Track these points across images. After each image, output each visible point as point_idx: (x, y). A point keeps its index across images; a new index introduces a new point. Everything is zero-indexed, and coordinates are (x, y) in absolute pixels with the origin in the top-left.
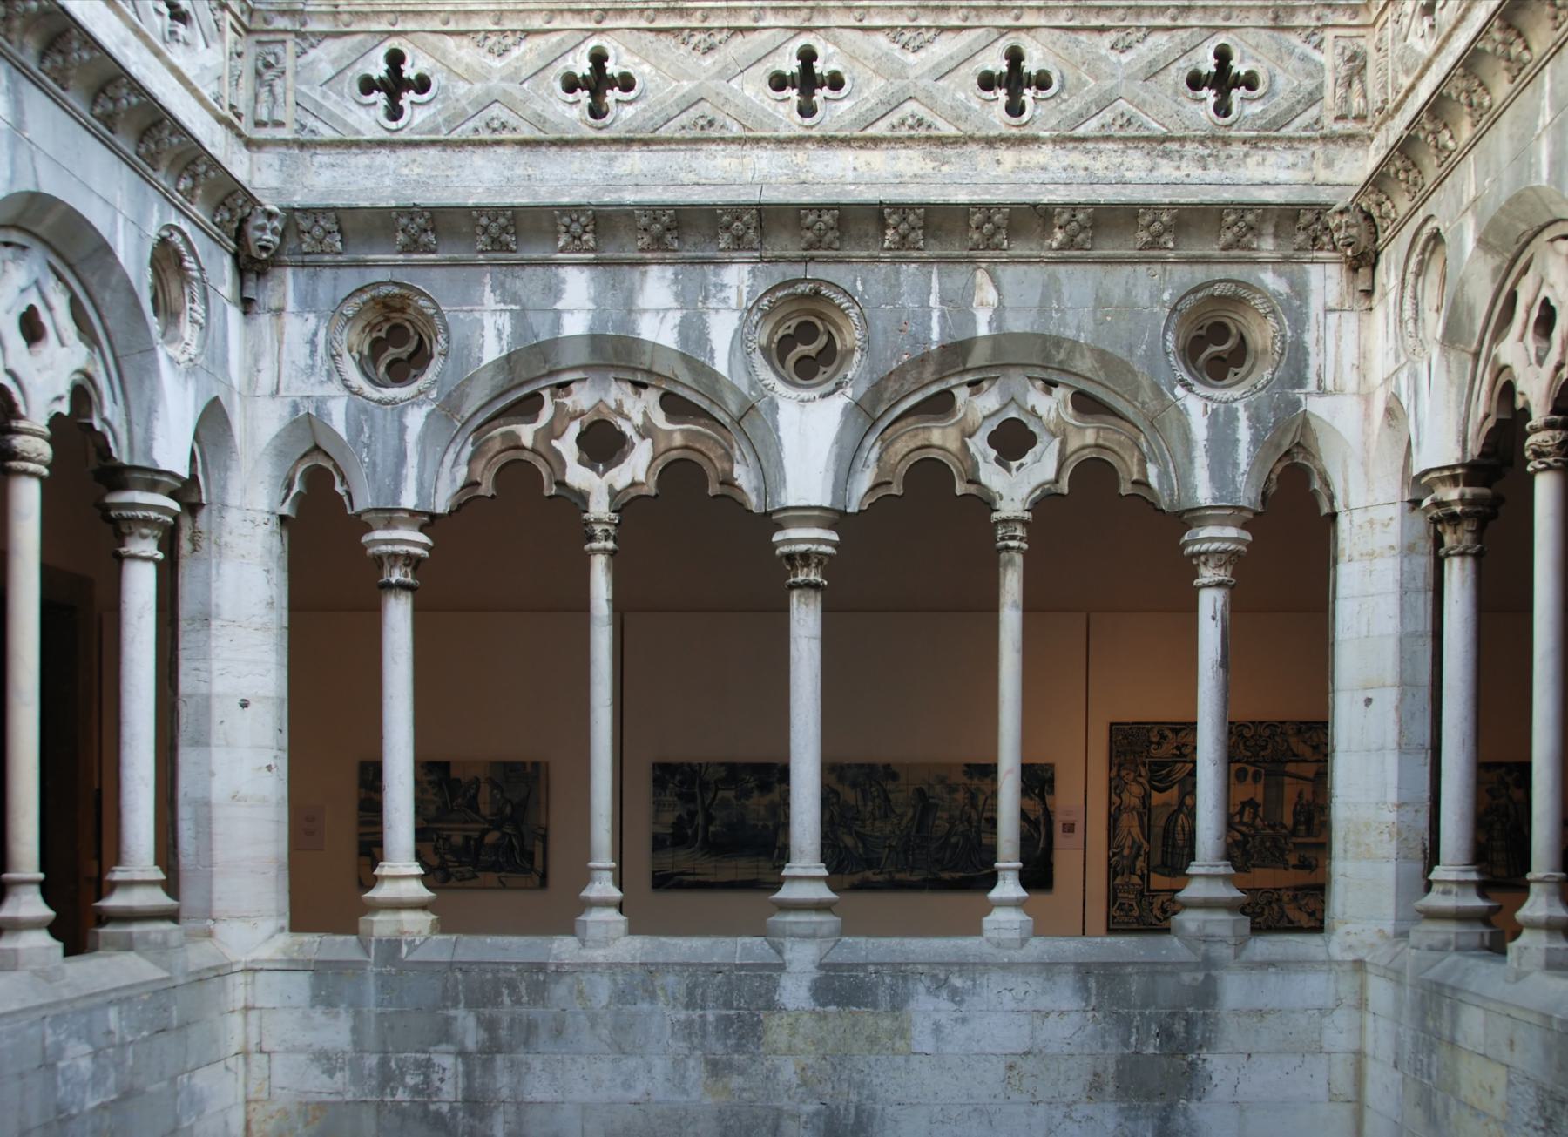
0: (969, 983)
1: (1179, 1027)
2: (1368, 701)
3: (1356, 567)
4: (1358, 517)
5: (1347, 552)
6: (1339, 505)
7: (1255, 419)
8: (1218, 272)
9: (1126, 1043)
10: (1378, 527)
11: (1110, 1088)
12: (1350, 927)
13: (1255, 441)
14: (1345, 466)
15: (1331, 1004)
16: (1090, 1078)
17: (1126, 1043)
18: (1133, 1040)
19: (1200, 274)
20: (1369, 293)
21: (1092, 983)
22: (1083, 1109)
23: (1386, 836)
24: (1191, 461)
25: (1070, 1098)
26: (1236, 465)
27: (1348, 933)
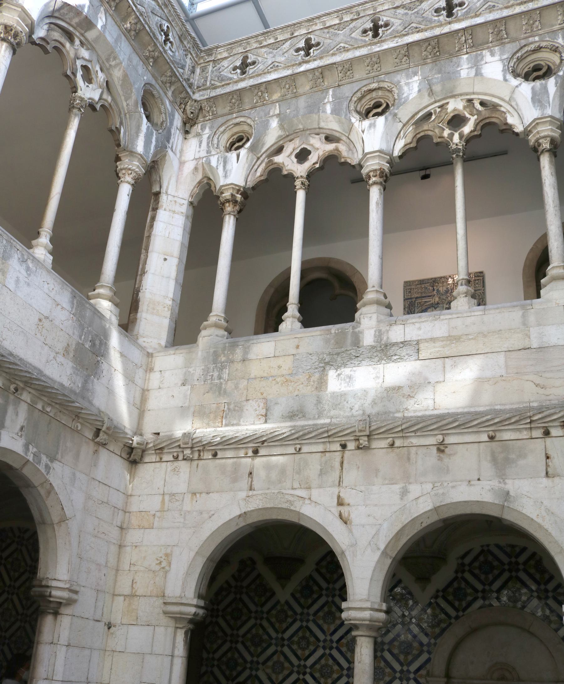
0: (34, 269)
1: (97, 342)
2: (165, 259)
3: (167, 213)
4: (170, 198)
5: (164, 207)
6: (163, 190)
7: (157, 141)
8: (157, 86)
9: (80, 338)
10: (178, 204)
11: (71, 355)
12: (145, 339)
13: (156, 147)
14: (170, 179)
15: (139, 364)
16: (66, 345)
17: (80, 338)
18: (83, 337)
19: (153, 82)
20: (187, 132)
21: (75, 302)
22: (60, 359)
23: (166, 309)
24: (138, 136)
25: (57, 350)
26: (150, 149)
27: (144, 342)
